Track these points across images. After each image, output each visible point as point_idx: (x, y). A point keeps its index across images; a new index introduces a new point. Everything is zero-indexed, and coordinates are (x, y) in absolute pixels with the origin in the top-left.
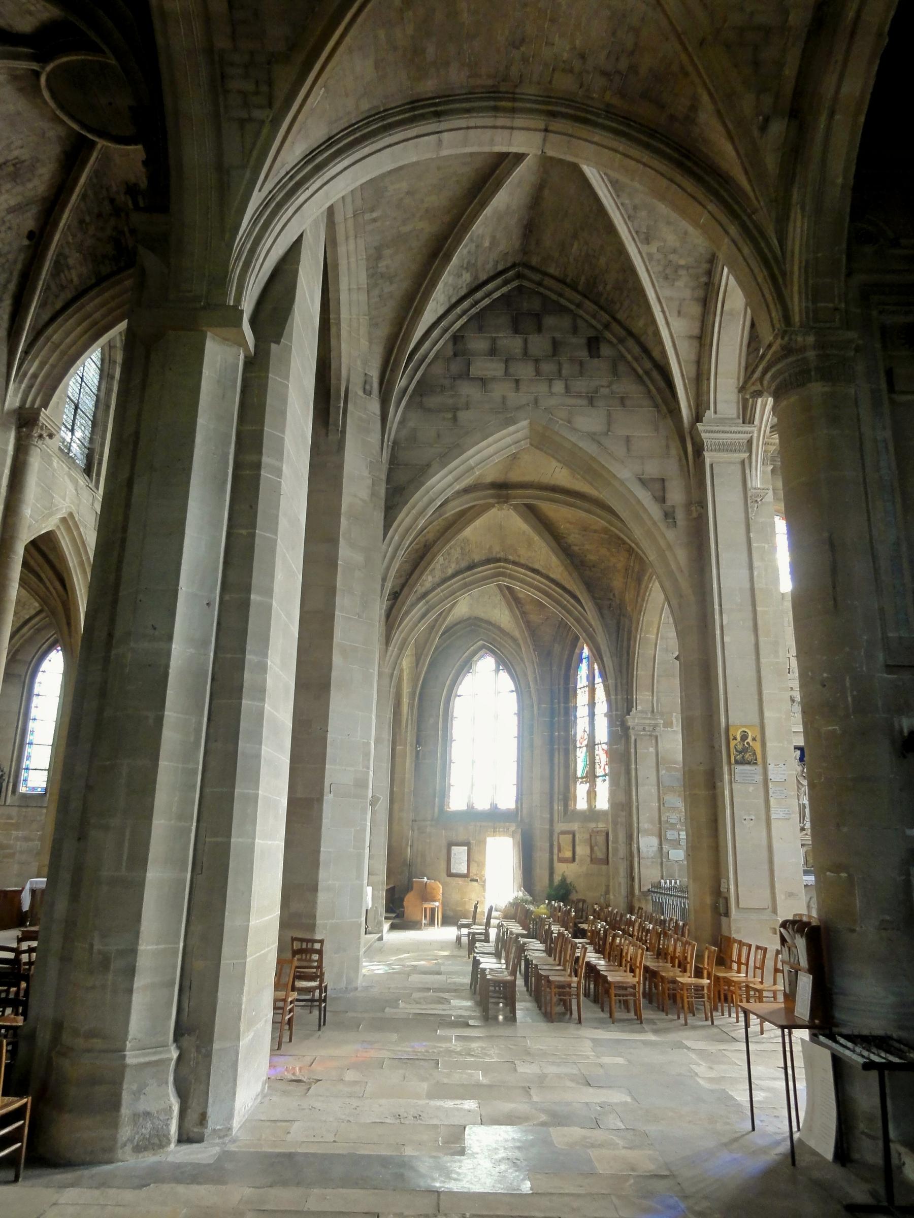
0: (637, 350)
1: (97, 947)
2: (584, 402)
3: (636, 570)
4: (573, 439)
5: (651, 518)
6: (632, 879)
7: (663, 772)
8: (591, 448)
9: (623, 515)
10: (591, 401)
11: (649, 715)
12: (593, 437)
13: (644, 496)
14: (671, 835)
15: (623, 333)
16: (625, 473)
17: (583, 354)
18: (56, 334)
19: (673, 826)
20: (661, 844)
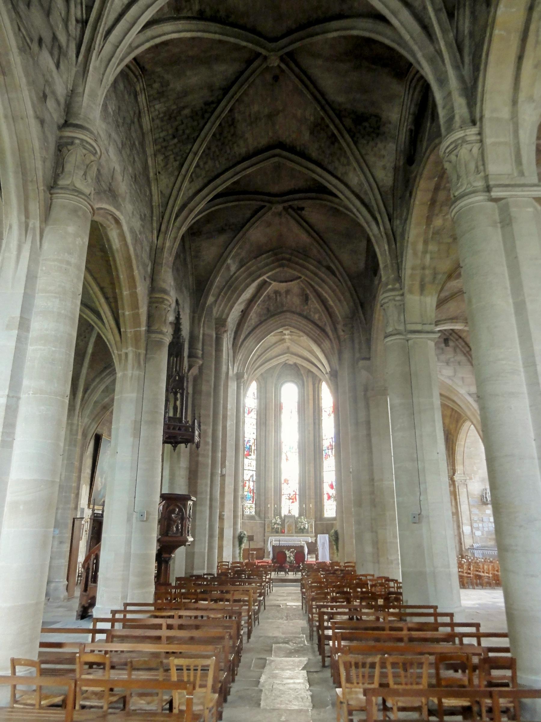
0: (463, 344)
2: (445, 364)
3: (456, 416)
5: (473, 408)
6: (461, 544)
7: (470, 499)
10: (448, 363)
11: (463, 475)
12: (449, 377)
13: (470, 400)
14: (475, 525)
15: (457, 337)
16: (463, 391)
18: (246, 344)
19: (476, 522)
20: (472, 529)
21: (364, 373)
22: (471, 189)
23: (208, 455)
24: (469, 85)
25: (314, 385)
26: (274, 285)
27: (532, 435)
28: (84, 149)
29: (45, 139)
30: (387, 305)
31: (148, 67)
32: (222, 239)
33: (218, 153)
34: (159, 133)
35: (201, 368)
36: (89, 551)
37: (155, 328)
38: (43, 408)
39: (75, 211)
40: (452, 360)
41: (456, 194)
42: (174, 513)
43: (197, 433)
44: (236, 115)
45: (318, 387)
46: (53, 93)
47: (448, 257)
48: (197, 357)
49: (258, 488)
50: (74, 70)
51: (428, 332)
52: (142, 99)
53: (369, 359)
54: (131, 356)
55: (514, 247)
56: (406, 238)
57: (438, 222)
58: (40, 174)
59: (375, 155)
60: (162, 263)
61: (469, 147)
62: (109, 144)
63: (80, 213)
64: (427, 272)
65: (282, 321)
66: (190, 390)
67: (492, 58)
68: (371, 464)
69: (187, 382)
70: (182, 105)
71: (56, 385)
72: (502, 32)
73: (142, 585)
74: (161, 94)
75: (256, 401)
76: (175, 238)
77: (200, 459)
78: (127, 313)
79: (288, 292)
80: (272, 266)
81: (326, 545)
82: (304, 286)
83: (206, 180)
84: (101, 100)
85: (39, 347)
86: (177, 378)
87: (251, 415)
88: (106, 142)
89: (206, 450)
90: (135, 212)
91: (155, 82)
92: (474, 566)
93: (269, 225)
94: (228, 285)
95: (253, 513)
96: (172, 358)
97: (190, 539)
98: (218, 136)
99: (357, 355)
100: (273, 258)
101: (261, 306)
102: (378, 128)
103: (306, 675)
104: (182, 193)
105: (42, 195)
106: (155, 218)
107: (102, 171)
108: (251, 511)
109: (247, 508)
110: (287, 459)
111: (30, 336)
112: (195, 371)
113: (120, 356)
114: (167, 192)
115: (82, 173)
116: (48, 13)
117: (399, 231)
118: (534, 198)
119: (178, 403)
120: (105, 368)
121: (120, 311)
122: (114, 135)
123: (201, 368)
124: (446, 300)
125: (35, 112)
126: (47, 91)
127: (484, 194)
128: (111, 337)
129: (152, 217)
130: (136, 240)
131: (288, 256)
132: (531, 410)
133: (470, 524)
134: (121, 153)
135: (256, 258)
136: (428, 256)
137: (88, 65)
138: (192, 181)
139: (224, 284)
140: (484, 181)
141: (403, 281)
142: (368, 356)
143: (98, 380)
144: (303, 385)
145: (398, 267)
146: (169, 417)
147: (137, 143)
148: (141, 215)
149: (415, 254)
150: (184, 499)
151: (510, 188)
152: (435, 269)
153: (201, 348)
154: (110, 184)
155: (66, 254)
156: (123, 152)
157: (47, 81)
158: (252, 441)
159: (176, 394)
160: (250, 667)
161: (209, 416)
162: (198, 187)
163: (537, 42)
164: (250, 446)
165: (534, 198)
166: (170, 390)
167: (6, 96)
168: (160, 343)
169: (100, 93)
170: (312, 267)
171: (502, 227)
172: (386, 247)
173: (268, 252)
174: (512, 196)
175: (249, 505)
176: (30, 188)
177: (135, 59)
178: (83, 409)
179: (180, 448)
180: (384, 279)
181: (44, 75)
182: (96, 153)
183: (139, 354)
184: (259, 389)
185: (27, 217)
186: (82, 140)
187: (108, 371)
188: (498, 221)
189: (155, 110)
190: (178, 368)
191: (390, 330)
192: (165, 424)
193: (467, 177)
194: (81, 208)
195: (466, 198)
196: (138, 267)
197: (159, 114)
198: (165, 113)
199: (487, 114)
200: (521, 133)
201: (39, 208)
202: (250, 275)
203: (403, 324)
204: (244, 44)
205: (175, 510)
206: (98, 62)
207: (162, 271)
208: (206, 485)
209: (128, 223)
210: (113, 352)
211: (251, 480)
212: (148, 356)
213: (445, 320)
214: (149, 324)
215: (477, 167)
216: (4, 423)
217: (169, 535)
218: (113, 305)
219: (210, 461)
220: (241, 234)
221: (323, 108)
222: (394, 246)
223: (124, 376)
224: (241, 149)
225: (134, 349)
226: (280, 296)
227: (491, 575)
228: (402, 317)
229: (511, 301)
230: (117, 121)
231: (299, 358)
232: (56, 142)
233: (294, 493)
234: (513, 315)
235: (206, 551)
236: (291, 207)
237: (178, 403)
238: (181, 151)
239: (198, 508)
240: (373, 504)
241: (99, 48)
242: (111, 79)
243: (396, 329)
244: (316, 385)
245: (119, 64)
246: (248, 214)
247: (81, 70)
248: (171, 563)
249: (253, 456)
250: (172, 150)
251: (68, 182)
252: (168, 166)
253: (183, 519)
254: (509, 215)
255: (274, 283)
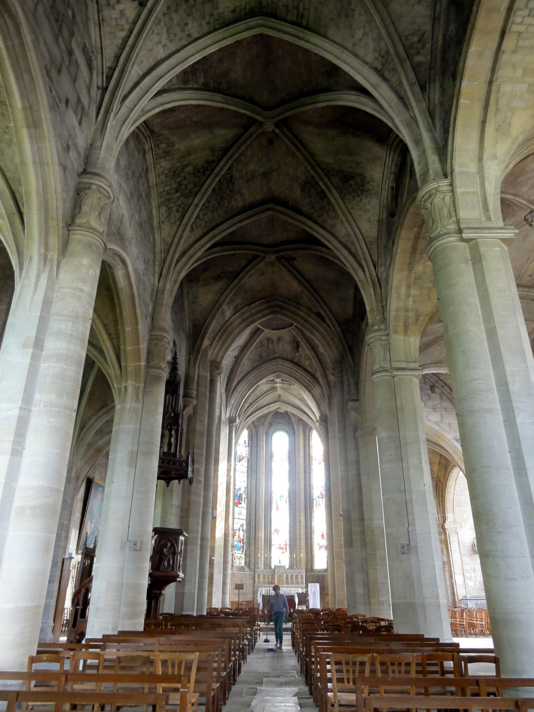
1: (380, 599)
2: (432, 410)
3: (445, 463)
4: (430, 424)
6: (454, 594)
7: (461, 548)
8: (436, 427)
9: (451, 452)
10: (434, 410)
12: (436, 423)
14: (467, 575)
15: (443, 384)
17: (429, 392)
18: (239, 388)
21: (353, 414)
22: (445, 231)
23: (200, 494)
24: (441, 145)
25: (304, 433)
26: (267, 333)
27: (507, 448)
28: (101, 193)
29: (66, 183)
30: (373, 344)
31: (156, 130)
32: (218, 286)
33: (216, 205)
34: (164, 187)
35: (195, 409)
36: (80, 585)
37: (154, 363)
38: (52, 419)
39: (89, 246)
40: (439, 406)
41: (432, 236)
42: (166, 547)
43: (190, 469)
44: (234, 173)
45: (309, 436)
46: (76, 145)
47: (429, 300)
48: (191, 397)
49: (249, 538)
50: (93, 128)
51: (412, 369)
52: (149, 156)
53: (358, 400)
54: (130, 389)
55: (484, 281)
56: (390, 283)
57: (419, 268)
58: (60, 213)
59: (360, 209)
60: (162, 304)
61: (441, 196)
62: (120, 193)
63: (94, 248)
64: (410, 314)
65: (274, 367)
66: (185, 428)
67: (459, 122)
68: (361, 504)
69: (182, 419)
70: (185, 163)
71: (65, 399)
72: (467, 101)
73: (132, 616)
74: (167, 153)
75: (247, 449)
76: (176, 281)
77: (192, 497)
78: (128, 348)
79: (279, 339)
80: (265, 312)
81: (316, 594)
82: (295, 333)
83: (205, 230)
84: (115, 153)
85: (51, 364)
86: (172, 415)
87: (241, 463)
88: (117, 191)
89: (198, 487)
90: (139, 256)
91: (162, 143)
92: (466, 613)
93: (263, 274)
94: (223, 329)
95: (243, 564)
96: (168, 396)
97: (181, 575)
98: (217, 191)
99: (346, 397)
100: (266, 305)
101: (253, 353)
102: (363, 185)
103: (297, 700)
104: (182, 241)
105: (61, 230)
106: (157, 263)
107: (112, 215)
108: (241, 561)
109: (236, 559)
110: (277, 509)
111: (44, 355)
112: (189, 411)
113: (120, 389)
114: (169, 240)
115: (97, 213)
116: (74, 80)
117: (383, 277)
118: (500, 239)
119: (173, 440)
120: (102, 407)
121: (121, 347)
122: (124, 186)
123: (195, 409)
124: (430, 344)
125: (59, 159)
126: (70, 142)
127: (457, 235)
128: (112, 372)
129: (154, 262)
130: (139, 280)
131: (281, 304)
132: (505, 425)
133: (462, 573)
134: (129, 202)
135: (249, 305)
136: (411, 299)
137: (106, 123)
138: (193, 230)
139: (219, 328)
140: (456, 225)
141: (388, 322)
142: (356, 398)
143: (94, 419)
144: (294, 433)
145: (383, 308)
146: (164, 453)
147: (143, 195)
148: (144, 259)
149: (398, 297)
150: (177, 533)
151: (478, 231)
152: (417, 311)
153: (195, 388)
154: (119, 228)
155: (80, 283)
156: (131, 201)
157: (70, 135)
158: (243, 489)
159: (170, 431)
160: (242, 694)
161: (202, 455)
162: (198, 236)
163: (497, 110)
164: (241, 494)
165: (500, 239)
166: (165, 425)
167: (36, 146)
168: (158, 378)
169: (115, 147)
170: (303, 314)
171: (473, 264)
172: (372, 292)
173: (262, 299)
174: (481, 238)
175: (239, 556)
176: (51, 224)
177: (145, 122)
178: (78, 447)
179: (173, 483)
180: (370, 321)
181: (68, 130)
182: (110, 197)
183: (138, 388)
184: (251, 437)
185: (47, 249)
186: (98, 186)
187: (104, 410)
188: (469, 258)
189: (161, 167)
190: (173, 405)
191: (376, 367)
192: (160, 459)
193: (441, 221)
194: (94, 243)
195: (441, 238)
196: (140, 306)
197: (165, 170)
198: (169, 169)
199: (457, 168)
200: (487, 184)
201: (58, 242)
202: (244, 321)
203: (389, 362)
204: (243, 111)
205: (167, 545)
206: (114, 122)
207: (163, 312)
208: (198, 524)
209: (133, 264)
210: (113, 385)
211: (241, 529)
212: (147, 389)
213: (430, 364)
214: (148, 361)
215: (449, 212)
216: (15, 433)
217: (160, 569)
218: (115, 341)
219: (202, 501)
220: (236, 281)
221: (313, 167)
222: (379, 291)
223: (123, 409)
224: (238, 203)
225: (133, 383)
226: (272, 342)
227: (484, 623)
228: (388, 355)
229: (483, 328)
230: (127, 175)
231: (289, 406)
232: (75, 187)
233: (285, 543)
234: (486, 340)
235: (196, 592)
236: (283, 257)
237: (173, 440)
238: (183, 203)
239: (189, 547)
240: (364, 544)
241: (116, 110)
242: (126, 136)
243: (382, 367)
244: (307, 434)
245: (132, 125)
246: (243, 263)
247: (100, 128)
248: (162, 599)
249: (244, 505)
250: (175, 203)
251: (85, 221)
252: (172, 216)
253: (174, 553)
254: (479, 253)
255: (267, 331)
